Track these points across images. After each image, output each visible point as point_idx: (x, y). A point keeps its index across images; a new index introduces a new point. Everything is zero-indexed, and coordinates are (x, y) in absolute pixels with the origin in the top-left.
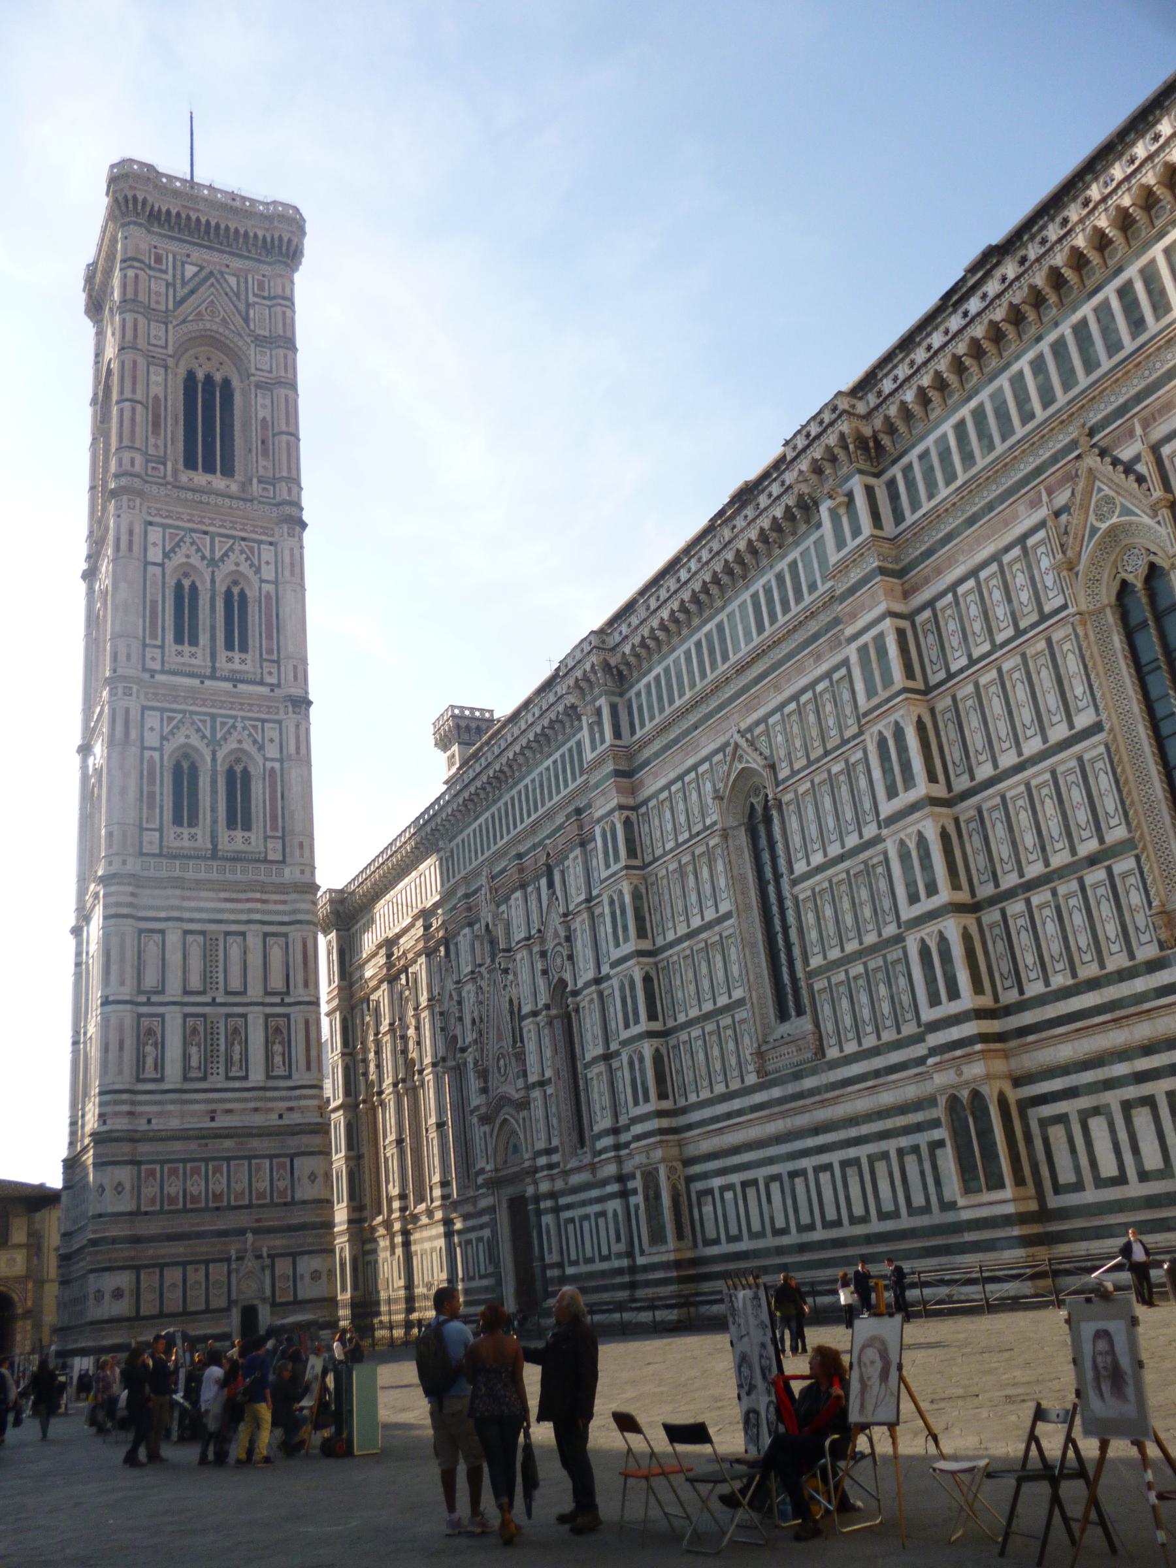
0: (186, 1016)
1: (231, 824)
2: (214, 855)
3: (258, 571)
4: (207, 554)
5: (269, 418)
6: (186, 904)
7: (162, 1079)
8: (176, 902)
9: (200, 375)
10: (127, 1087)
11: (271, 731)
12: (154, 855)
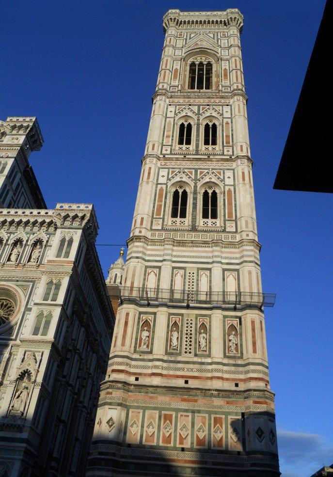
1: (205, 216)
2: (194, 229)
3: (222, 114)
4: (196, 112)
5: (228, 68)
6: (174, 253)
7: (151, 352)
8: (170, 252)
9: (197, 63)
10: (126, 354)
11: (229, 174)
12: (158, 230)
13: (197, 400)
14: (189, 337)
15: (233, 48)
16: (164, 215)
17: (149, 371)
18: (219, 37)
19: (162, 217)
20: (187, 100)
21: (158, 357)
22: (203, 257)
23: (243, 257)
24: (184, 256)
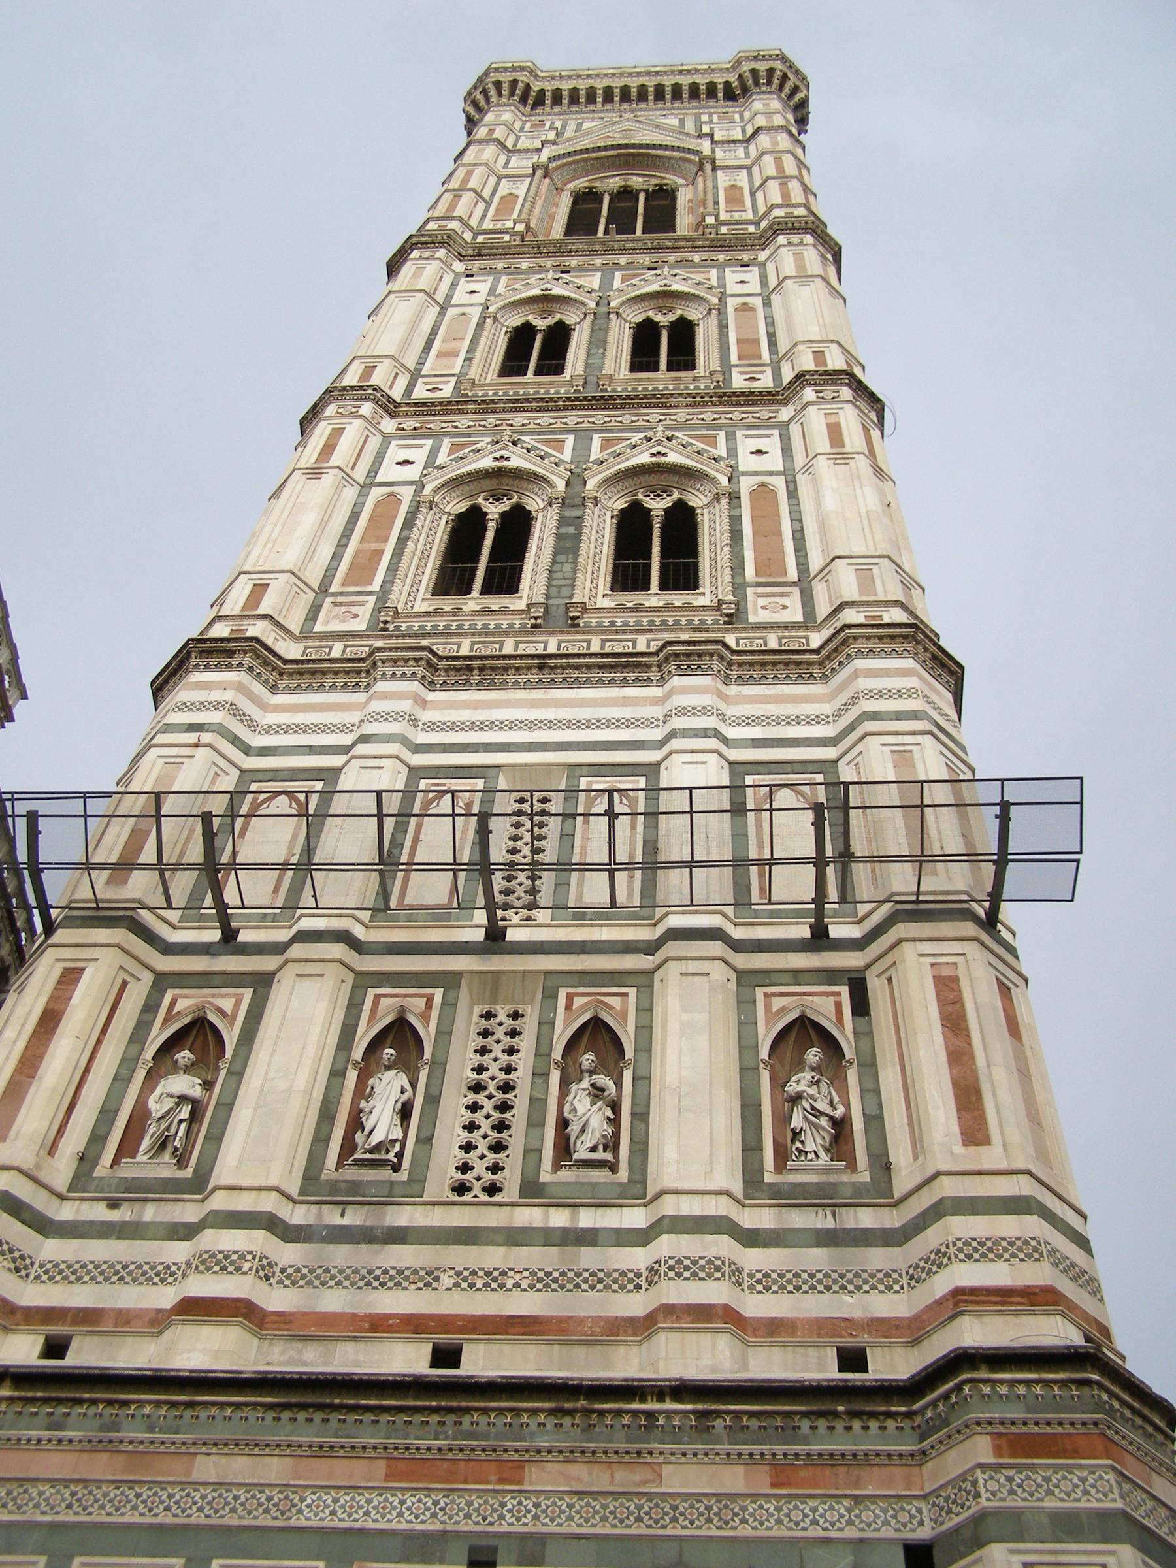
0: (364, 981)
13: (520, 1465)
14: (488, 1106)
15: (764, 140)
16: (387, 583)
17: (165, 1297)
18: (705, 118)
19: (376, 586)
20: (550, 262)
21: (245, 1203)
22: (608, 724)
23: (854, 700)
24: (491, 725)
